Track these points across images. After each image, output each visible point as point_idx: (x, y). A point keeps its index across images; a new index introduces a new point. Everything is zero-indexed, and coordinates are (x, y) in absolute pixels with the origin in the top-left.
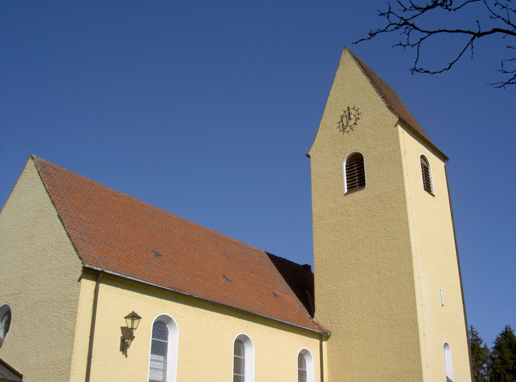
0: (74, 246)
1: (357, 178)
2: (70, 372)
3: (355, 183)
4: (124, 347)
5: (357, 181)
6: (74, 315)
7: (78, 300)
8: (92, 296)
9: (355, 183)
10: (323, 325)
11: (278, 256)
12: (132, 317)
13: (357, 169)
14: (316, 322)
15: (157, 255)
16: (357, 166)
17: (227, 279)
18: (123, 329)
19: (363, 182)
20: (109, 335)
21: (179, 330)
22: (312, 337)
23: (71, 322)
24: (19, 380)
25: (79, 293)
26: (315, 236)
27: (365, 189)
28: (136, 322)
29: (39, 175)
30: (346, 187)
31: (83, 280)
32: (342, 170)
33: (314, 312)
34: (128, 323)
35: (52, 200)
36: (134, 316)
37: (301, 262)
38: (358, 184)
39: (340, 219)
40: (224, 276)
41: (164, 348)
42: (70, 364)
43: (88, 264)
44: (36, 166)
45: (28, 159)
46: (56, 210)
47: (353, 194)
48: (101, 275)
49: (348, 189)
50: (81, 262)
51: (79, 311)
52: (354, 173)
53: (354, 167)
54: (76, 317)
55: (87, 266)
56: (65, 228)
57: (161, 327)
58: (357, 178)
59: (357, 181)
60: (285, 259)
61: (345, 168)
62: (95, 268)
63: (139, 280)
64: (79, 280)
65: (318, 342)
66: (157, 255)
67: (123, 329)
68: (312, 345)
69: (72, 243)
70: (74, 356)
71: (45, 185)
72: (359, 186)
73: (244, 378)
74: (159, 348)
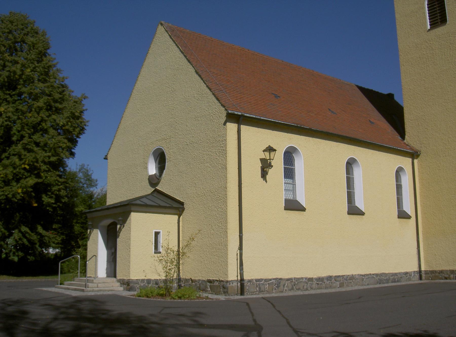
0: (215, 96)
1: (438, 15)
2: (226, 197)
3: (437, 20)
4: (264, 175)
5: (439, 17)
6: (224, 152)
7: (226, 140)
8: (236, 136)
9: (437, 20)
10: (413, 146)
11: (366, 87)
12: (269, 150)
13: (438, 7)
14: (407, 143)
15: (276, 96)
16: (438, 4)
17: (332, 112)
18: (261, 160)
19: (430, 15)
20: (252, 168)
21: (304, 157)
22: (405, 156)
23: (222, 158)
24: (182, 206)
25: (226, 134)
26: (402, 69)
27: (447, 24)
28: (272, 154)
29: (171, 38)
30: (429, 23)
31: (228, 124)
32: (424, 8)
33: (405, 135)
34: (266, 155)
35: (187, 59)
36: (270, 149)
37: (385, 91)
38: (439, 20)
39: (425, 53)
40: (329, 110)
41: (293, 172)
42: (226, 191)
43: (231, 110)
44: (167, 31)
45: (158, 25)
46: (193, 67)
47: (436, 30)
48: (241, 118)
49: (430, 25)
50: (224, 109)
51: (228, 149)
52: (436, 11)
53: (435, 5)
54: (226, 154)
55: (230, 112)
56: (204, 82)
57: (289, 156)
58: (438, 15)
59: (439, 17)
60: (372, 90)
61: (427, 6)
62: (236, 113)
63: (270, 120)
64: (225, 124)
65: (410, 160)
66: (276, 96)
67: (261, 160)
68: (405, 162)
69: (213, 94)
70: (228, 185)
71: (178, 47)
72: (441, 22)
73: (354, 193)
74: (289, 173)
